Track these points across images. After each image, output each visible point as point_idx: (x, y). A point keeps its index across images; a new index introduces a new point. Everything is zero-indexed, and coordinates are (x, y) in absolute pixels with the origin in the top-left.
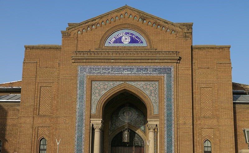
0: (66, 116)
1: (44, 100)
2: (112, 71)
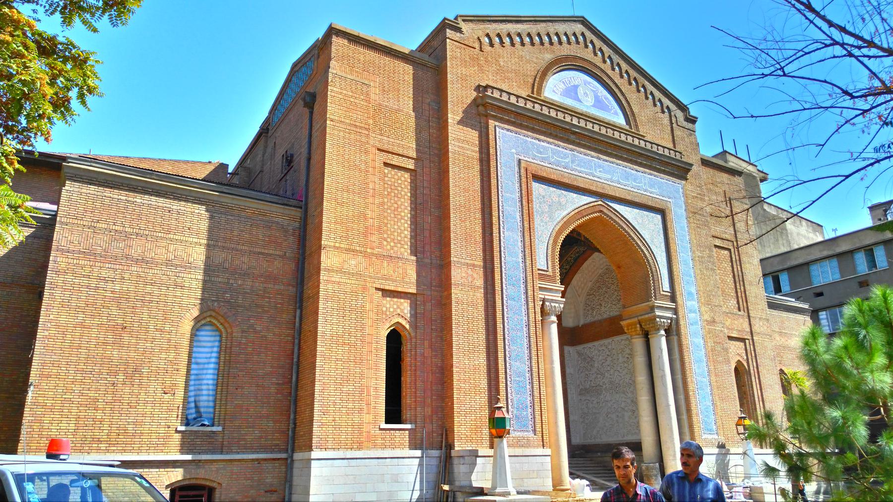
0: (474, 265)
1: (396, 206)
2: (573, 162)
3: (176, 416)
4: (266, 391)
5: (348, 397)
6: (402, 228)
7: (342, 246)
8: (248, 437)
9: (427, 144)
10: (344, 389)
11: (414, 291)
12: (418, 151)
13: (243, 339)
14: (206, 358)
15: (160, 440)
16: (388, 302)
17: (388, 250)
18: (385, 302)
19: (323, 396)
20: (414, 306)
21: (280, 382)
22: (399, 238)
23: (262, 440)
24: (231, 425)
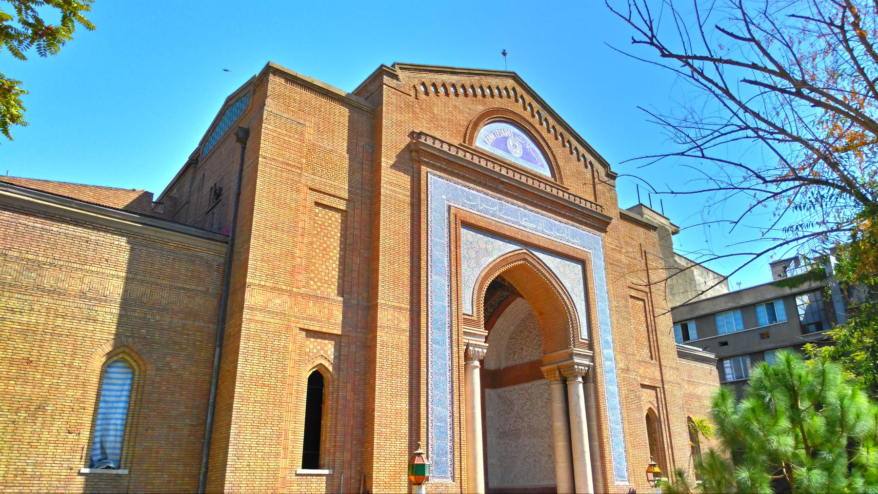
0: (400, 308)
1: (325, 245)
2: (500, 210)
3: (79, 457)
4: (178, 432)
5: (265, 441)
6: (330, 268)
7: (268, 284)
8: (156, 482)
9: (359, 186)
10: (261, 433)
11: (340, 333)
12: (350, 192)
13: (157, 378)
14: (116, 396)
15: (61, 483)
16: (313, 344)
17: (315, 290)
18: (308, 343)
19: (238, 439)
20: (338, 348)
21: (193, 423)
22: (327, 278)
23: (171, 484)
24: (138, 468)
